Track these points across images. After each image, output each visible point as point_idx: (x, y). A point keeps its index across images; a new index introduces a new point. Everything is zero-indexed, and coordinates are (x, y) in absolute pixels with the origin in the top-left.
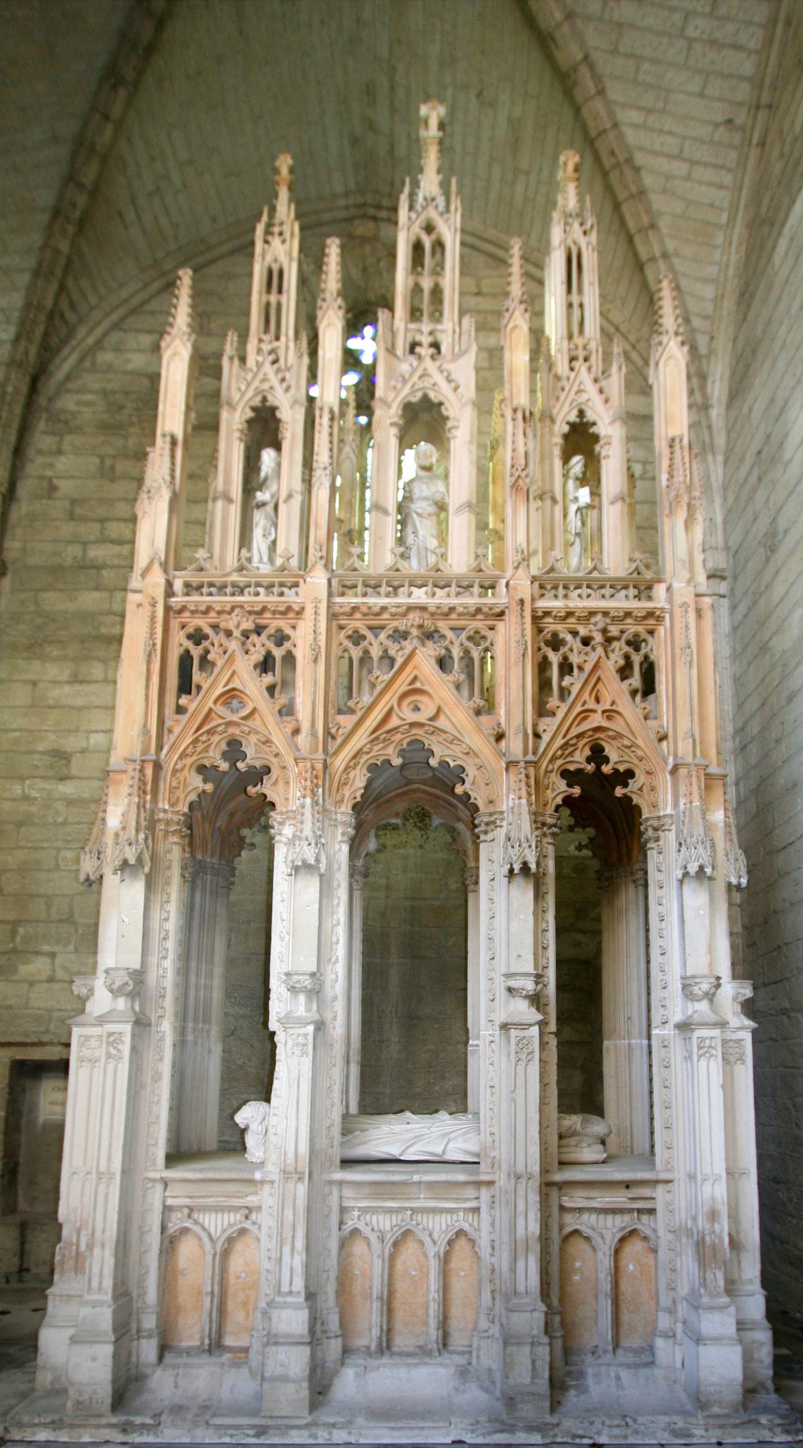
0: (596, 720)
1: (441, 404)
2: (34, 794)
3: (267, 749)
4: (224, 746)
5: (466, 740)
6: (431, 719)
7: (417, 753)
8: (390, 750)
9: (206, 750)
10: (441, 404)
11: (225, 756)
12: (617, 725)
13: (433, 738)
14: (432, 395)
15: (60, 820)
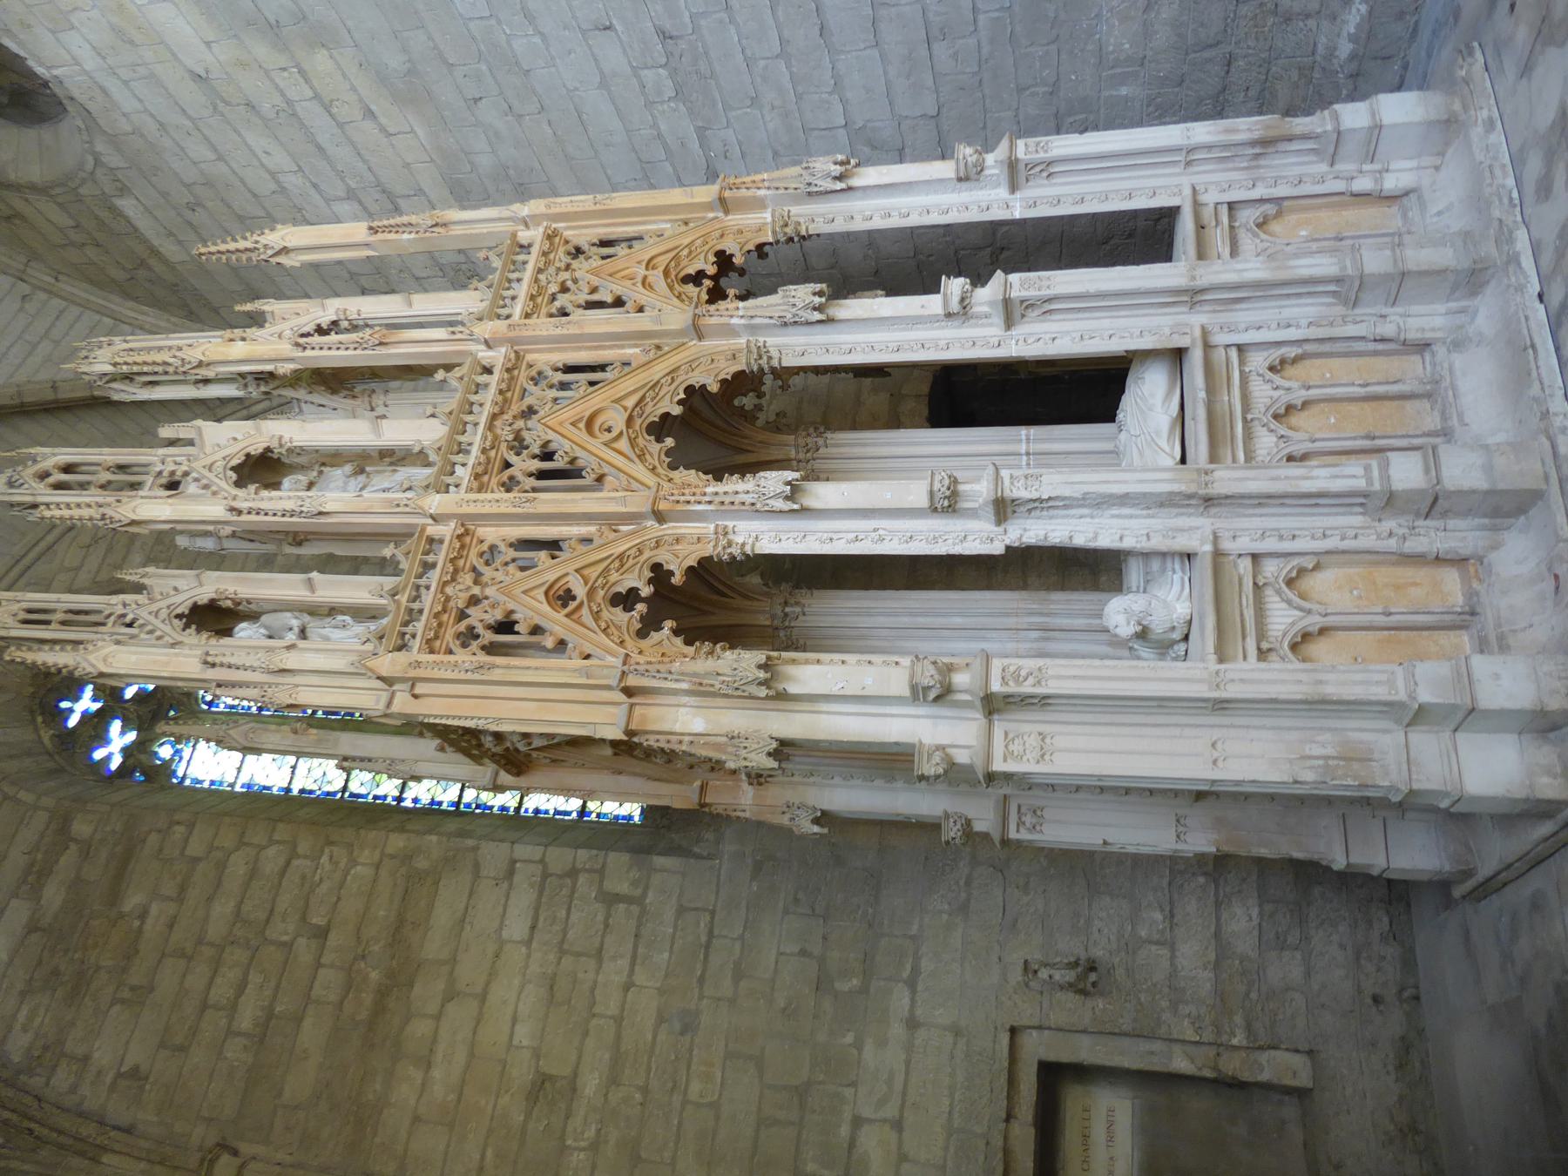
0: (656, 276)
1: (248, 455)
2: (591, 1133)
3: (631, 562)
4: (618, 610)
5: (656, 378)
6: (625, 409)
7: (660, 428)
8: (655, 448)
9: (619, 628)
10: (248, 455)
11: (628, 608)
12: (662, 262)
13: (648, 409)
14: (235, 462)
15: (638, 1096)
